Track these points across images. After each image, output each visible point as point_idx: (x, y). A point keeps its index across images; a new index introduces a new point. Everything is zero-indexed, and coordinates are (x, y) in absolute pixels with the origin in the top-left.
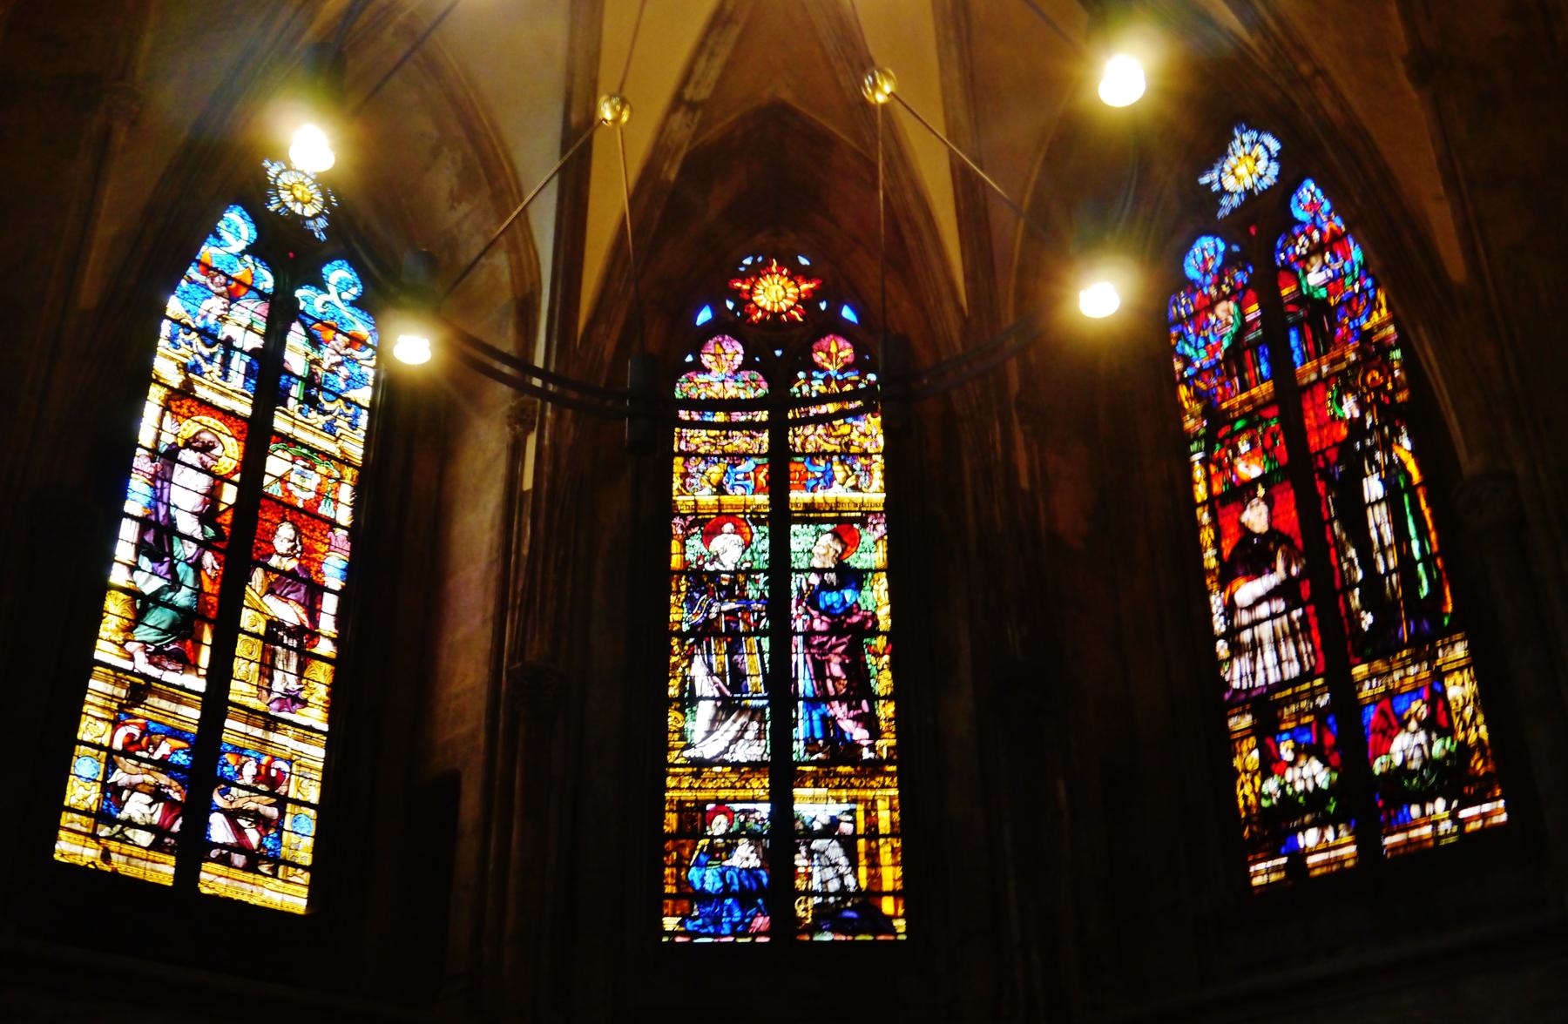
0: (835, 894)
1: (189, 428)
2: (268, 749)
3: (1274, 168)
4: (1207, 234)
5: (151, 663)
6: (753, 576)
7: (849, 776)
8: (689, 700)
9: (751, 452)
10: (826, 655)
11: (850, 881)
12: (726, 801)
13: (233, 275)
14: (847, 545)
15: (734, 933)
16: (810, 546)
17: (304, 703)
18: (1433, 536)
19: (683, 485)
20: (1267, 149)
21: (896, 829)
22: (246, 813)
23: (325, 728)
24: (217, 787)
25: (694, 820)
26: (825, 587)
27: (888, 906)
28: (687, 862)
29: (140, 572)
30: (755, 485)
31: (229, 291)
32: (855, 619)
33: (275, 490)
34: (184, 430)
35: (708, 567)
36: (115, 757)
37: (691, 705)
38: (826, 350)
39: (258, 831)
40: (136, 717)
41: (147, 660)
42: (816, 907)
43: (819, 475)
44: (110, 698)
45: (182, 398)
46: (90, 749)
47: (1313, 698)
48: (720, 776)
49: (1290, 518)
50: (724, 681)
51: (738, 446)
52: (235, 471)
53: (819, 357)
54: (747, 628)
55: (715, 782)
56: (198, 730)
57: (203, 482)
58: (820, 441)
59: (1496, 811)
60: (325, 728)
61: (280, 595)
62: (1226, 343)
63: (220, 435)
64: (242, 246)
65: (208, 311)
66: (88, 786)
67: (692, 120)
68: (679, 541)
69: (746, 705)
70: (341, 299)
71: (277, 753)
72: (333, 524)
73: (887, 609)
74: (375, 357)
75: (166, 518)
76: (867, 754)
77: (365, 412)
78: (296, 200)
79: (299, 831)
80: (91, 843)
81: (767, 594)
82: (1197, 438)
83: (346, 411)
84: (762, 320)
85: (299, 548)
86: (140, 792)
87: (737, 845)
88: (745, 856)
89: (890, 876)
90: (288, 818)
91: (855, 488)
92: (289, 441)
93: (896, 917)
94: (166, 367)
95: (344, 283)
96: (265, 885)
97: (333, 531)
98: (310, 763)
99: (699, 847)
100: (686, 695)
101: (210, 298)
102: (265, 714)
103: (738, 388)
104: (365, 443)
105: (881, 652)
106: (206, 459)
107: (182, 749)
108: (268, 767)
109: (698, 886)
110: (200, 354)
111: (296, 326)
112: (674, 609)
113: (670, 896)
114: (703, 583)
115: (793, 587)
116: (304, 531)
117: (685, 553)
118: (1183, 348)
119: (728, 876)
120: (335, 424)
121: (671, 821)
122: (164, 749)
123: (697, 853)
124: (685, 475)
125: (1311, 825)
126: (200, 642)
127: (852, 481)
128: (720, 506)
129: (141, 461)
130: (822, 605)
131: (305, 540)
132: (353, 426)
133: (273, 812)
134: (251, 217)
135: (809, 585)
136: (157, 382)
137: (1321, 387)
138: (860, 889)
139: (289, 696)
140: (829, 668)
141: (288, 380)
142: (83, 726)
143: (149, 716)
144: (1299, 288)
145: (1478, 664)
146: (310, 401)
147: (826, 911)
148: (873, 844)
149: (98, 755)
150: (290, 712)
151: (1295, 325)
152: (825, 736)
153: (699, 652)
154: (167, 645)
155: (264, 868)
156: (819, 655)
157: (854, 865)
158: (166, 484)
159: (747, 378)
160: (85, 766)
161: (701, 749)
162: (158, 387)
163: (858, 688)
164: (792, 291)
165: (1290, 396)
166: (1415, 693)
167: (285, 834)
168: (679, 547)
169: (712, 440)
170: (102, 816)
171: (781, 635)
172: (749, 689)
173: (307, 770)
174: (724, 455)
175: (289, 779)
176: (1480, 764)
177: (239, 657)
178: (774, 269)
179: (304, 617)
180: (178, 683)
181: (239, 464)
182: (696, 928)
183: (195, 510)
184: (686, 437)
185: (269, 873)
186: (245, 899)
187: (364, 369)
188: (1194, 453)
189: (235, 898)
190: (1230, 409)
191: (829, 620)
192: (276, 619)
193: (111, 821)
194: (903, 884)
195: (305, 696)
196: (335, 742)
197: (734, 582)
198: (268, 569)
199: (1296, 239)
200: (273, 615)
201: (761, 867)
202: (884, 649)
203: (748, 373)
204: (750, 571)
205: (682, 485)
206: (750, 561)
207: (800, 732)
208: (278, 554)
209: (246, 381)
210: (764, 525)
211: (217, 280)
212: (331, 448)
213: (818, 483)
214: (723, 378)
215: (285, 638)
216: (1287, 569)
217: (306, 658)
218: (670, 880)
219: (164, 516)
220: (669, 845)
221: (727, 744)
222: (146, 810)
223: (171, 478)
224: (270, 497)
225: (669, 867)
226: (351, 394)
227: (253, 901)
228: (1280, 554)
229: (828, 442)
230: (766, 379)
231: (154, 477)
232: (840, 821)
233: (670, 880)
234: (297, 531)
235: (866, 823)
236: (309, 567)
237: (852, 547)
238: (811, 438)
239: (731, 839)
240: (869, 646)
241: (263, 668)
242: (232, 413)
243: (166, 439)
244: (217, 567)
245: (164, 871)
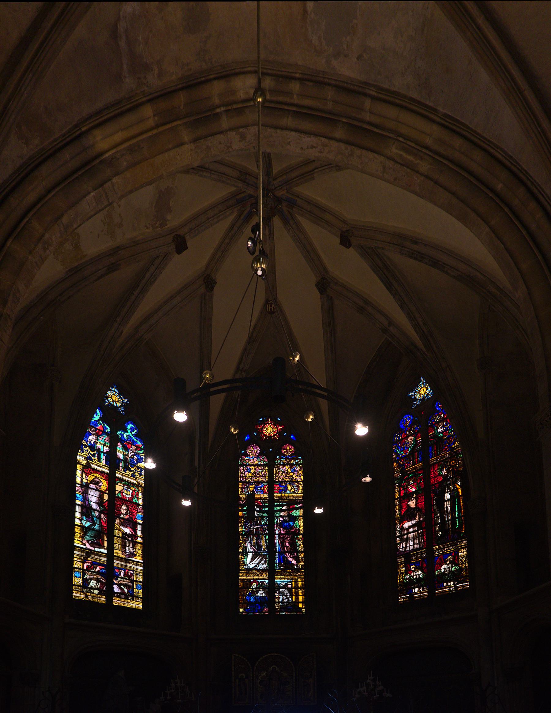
1: (91, 477)
2: (127, 568)
5: (90, 546)
17: (136, 555)
22: (123, 585)
24: (114, 578)
33: (119, 495)
34: (89, 478)
39: (127, 589)
52: (106, 490)
57: (97, 493)
63: (100, 479)
66: (79, 579)
72: (138, 504)
78: (113, 401)
85: (129, 512)
92: (121, 480)
102: (125, 558)
106: (97, 487)
107: (103, 568)
108: (128, 572)
120: (135, 474)
122: (98, 569)
131: (130, 510)
141: (119, 461)
142: (74, 563)
146: (126, 468)
154: (95, 541)
158: (87, 495)
177: (115, 543)
179: (132, 531)
183: (97, 502)
187: (142, 457)
195: (136, 553)
208: (123, 514)
217: (135, 543)
222: (95, 585)
224: (118, 497)
242: (103, 472)
244: (105, 518)
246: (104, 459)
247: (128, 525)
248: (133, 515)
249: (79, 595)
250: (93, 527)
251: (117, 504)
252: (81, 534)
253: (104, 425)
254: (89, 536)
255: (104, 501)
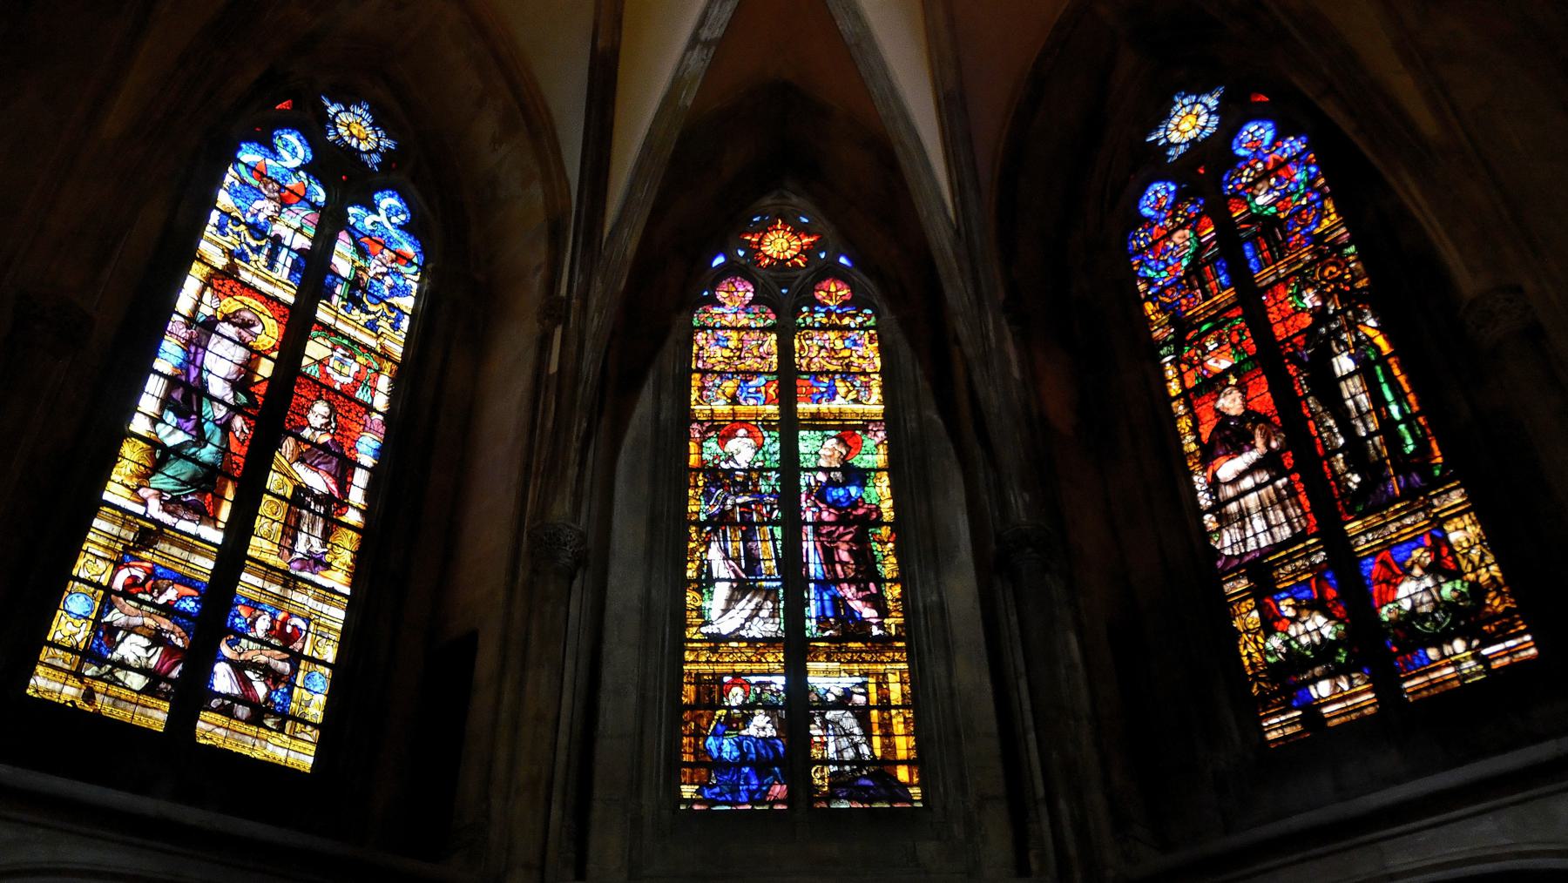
0: (850, 763)
1: (230, 305)
2: (286, 606)
3: (1215, 120)
4: (1158, 181)
5: (165, 510)
6: (765, 474)
7: (860, 651)
8: (706, 581)
9: (762, 370)
10: (834, 542)
11: (864, 749)
12: (742, 674)
13: (287, 185)
14: (851, 448)
15: (751, 801)
16: (816, 449)
17: (328, 566)
18: (1411, 398)
19: (701, 397)
20: (1206, 106)
21: (907, 701)
22: (255, 666)
23: (347, 591)
24: (226, 636)
25: (711, 692)
26: (832, 483)
27: (903, 774)
28: (704, 732)
29: (163, 425)
30: (766, 398)
31: (281, 197)
32: (861, 511)
33: (314, 371)
34: (225, 306)
35: (723, 465)
36: (113, 596)
37: (708, 587)
38: (827, 290)
39: (266, 685)
40: (143, 560)
41: (161, 507)
42: (832, 775)
43: (823, 390)
44: (115, 539)
45: (224, 279)
46: (86, 586)
47: (1308, 556)
48: (736, 651)
49: (1263, 400)
50: (739, 565)
51: (749, 365)
52: (273, 349)
53: (821, 295)
54: (760, 518)
55: (731, 656)
56: (210, 580)
57: (240, 354)
58: (824, 363)
59: (1525, 646)
60: (347, 591)
61: (310, 464)
62: (1185, 262)
63: (261, 316)
64: (297, 163)
65: (259, 210)
66: (77, 623)
67: (707, 55)
68: (697, 443)
69: (761, 586)
70: (390, 222)
71: (292, 609)
72: (369, 408)
73: (890, 503)
74: (419, 274)
75: (197, 380)
76: (876, 631)
77: (407, 317)
78: (352, 136)
79: (312, 688)
80: (72, 681)
81: (778, 489)
82: (1166, 343)
83: (389, 314)
84: (769, 265)
85: (333, 425)
86: (137, 634)
87: (753, 715)
88: (761, 725)
89: (903, 746)
90: (301, 675)
91: (856, 401)
92: (329, 330)
93: (911, 785)
94: (212, 249)
95: (394, 210)
96: (269, 739)
97: (369, 415)
98: (329, 623)
99: (716, 717)
100: (703, 577)
101: (262, 200)
102: (285, 572)
103: (749, 319)
104: (405, 344)
105: (886, 540)
106: (244, 334)
107: (192, 596)
108: (284, 623)
109: (716, 754)
110: (248, 245)
111: (343, 235)
112: (692, 502)
113: (688, 764)
114: (717, 479)
115: (802, 483)
116: (340, 411)
117: (702, 453)
118: (1145, 272)
119: (744, 745)
120: (378, 323)
121: (689, 693)
122: (171, 594)
123: (714, 723)
124: (702, 389)
125: (1322, 678)
126: (222, 498)
127: (852, 395)
128: (734, 414)
129: (176, 325)
130: (829, 499)
131: (339, 418)
132: (395, 327)
133: (286, 668)
134: (308, 141)
135: (817, 482)
136: (201, 260)
137: (1281, 287)
138: (875, 757)
139: (311, 558)
140: (838, 553)
141: (334, 280)
142: (80, 562)
143: (158, 562)
144: (1249, 210)
145: (1479, 507)
146: (354, 301)
147: (842, 779)
148: (886, 715)
149: (95, 592)
150: (312, 573)
151: (1249, 239)
152: (836, 615)
153: (716, 539)
154: (186, 496)
155: (269, 723)
156: (828, 542)
157: (868, 735)
158: (200, 350)
159: (757, 311)
160: (77, 602)
161: (718, 626)
162: (201, 265)
163: (866, 571)
164: (795, 243)
165: (1250, 300)
166: (1416, 541)
167: (296, 689)
168: (697, 449)
169: (726, 360)
170: (89, 654)
171: (793, 525)
172: (763, 572)
173: (326, 630)
174: (738, 372)
175: (306, 637)
176: (1496, 602)
177: (262, 516)
178: (779, 227)
179: (333, 487)
180: (193, 533)
181: (278, 344)
182: (713, 796)
183: (229, 377)
184: (703, 357)
185: (274, 728)
186: (246, 752)
187: (408, 282)
188: (1164, 356)
189: (235, 750)
190: (1194, 316)
191: (836, 513)
192: (304, 486)
193: (100, 660)
194: (918, 753)
195: (329, 560)
196: (355, 605)
197: (748, 478)
198: (299, 438)
199: (1242, 171)
200: (300, 481)
201: (778, 737)
202: (889, 538)
203: (758, 307)
204: (761, 469)
205: (699, 397)
206: (762, 461)
207: (812, 610)
208: (311, 427)
209: (290, 274)
210: (774, 430)
211: (270, 186)
212: (372, 343)
213: (822, 397)
214: (736, 310)
215: (313, 504)
216: (1267, 444)
217: (332, 525)
218: (687, 749)
219: (195, 378)
220: (687, 715)
221: (743, 621)
222: (142, 653)
223: (207, 345)
224: (308, 377)
225: (687, 736)
226: (395, 301)
227: (254, 755)
228: (1257, 432)
229: (830, 363)
230: (774, 312)
231: (188, 342)
232: (853, 693)
233: (687, 749)
234: (332, 409)
235: (878, 695)
236: (342, 443)
237: (856, 449)
238: (815, 360)
239: (748, 710)
240: (874, 534)
241: (287, 529)
242: (276, 299)
243: (206, 310)
244: (247, 431)
245: (156, 716)
246: (289, 263)
247: (324, 463)
248: (348, 437)
249: (58, 687)
250: (193, 450)
251: (299, 395)
252: (139, 464)
253: (309, 183)
254: (169, 476)
255: (257, 379)
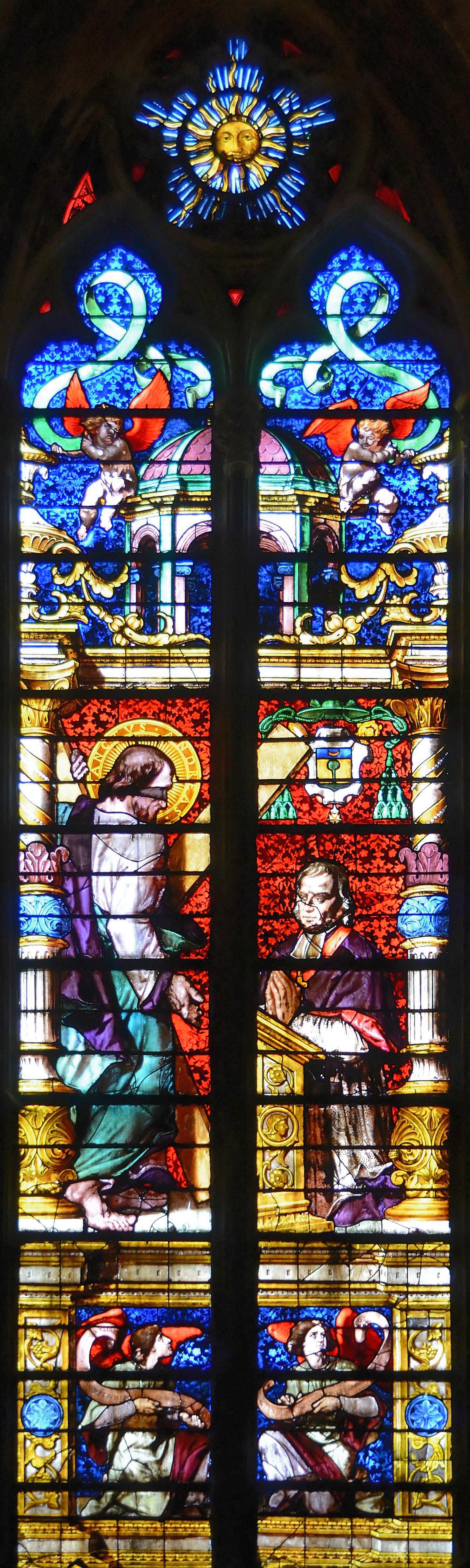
40: (107, 1308)
46: (41, 1382)
66: (49, 1442)
107: (192, 1338)
122: (161, 1347)
193: (96, 1489)
222: (146, 1457)
